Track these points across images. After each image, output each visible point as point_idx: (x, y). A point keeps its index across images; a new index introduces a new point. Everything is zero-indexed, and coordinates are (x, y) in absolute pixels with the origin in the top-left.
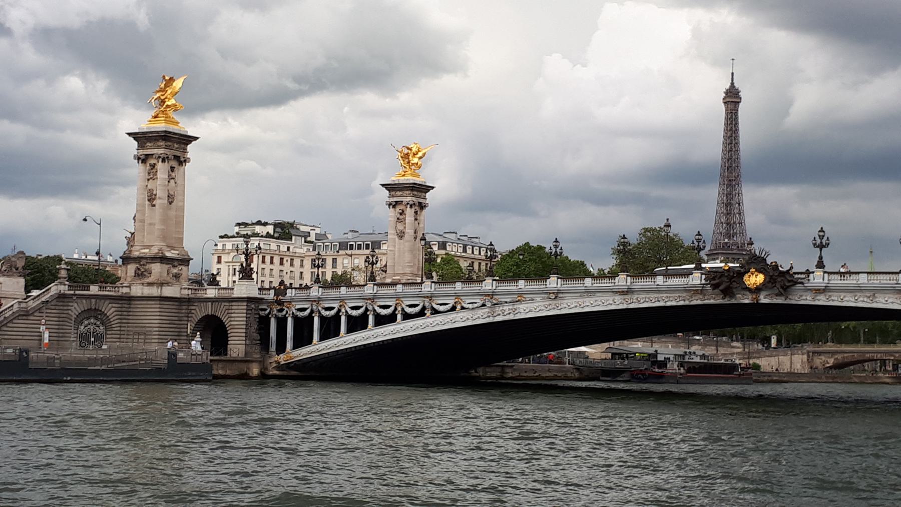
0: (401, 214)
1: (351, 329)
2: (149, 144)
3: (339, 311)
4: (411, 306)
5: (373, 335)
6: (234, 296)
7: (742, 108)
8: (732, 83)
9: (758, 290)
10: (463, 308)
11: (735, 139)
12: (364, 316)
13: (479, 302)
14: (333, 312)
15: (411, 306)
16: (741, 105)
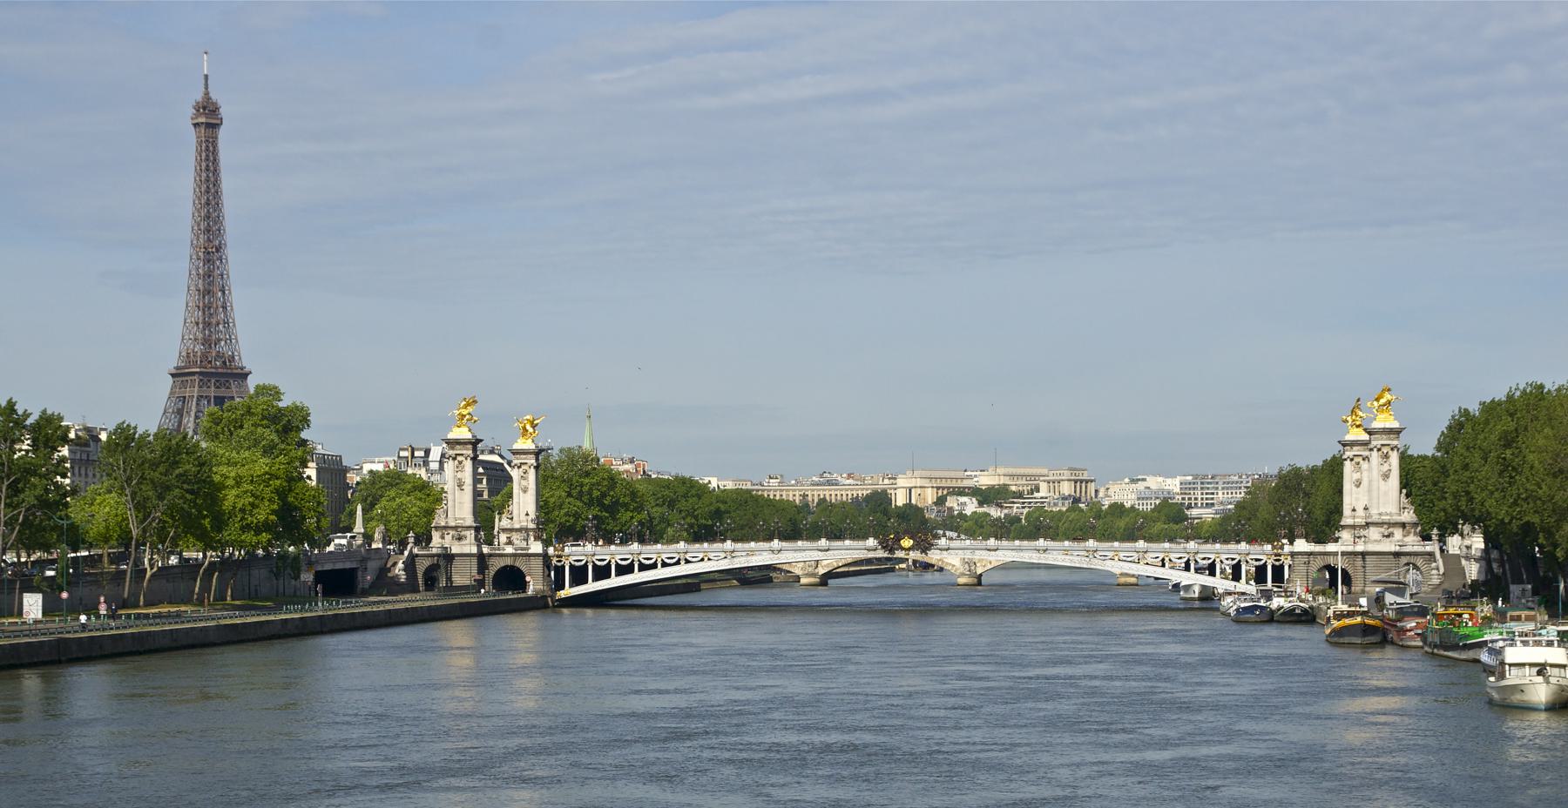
0: (525, 473)
1: (618, 574)
2: (458, 446)
3: (610, 561)
4: (668, 558)
5: (636, 577)
6: (530, 551)
7: (223, 134)
8: (207, 94)
9: (909, 549)
10: (709, 559)
11: (214, 185)
12: (632, 564)
13: (723, 555)
14: (605, 563)
15: (668, 558)
16: (222, 128)
